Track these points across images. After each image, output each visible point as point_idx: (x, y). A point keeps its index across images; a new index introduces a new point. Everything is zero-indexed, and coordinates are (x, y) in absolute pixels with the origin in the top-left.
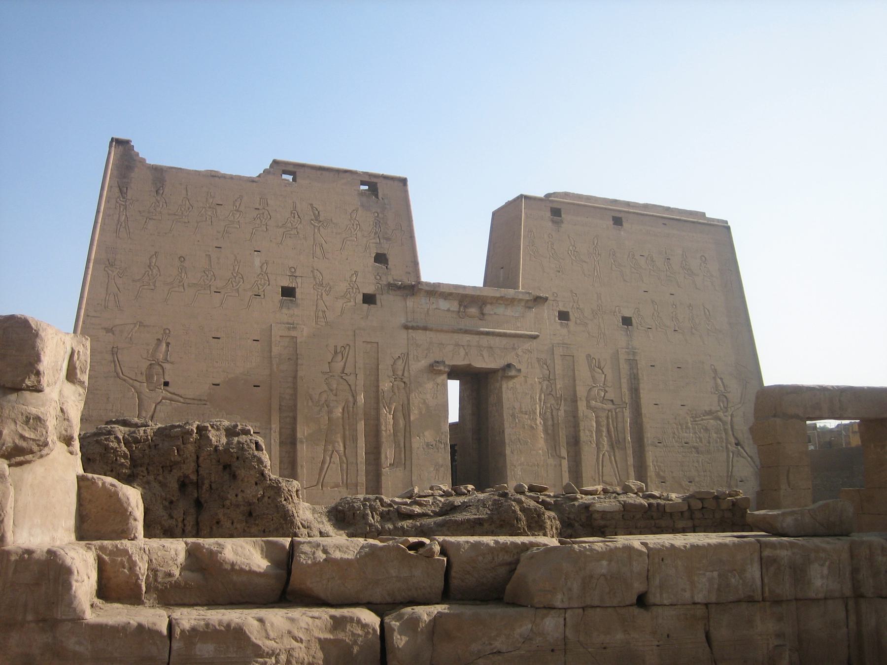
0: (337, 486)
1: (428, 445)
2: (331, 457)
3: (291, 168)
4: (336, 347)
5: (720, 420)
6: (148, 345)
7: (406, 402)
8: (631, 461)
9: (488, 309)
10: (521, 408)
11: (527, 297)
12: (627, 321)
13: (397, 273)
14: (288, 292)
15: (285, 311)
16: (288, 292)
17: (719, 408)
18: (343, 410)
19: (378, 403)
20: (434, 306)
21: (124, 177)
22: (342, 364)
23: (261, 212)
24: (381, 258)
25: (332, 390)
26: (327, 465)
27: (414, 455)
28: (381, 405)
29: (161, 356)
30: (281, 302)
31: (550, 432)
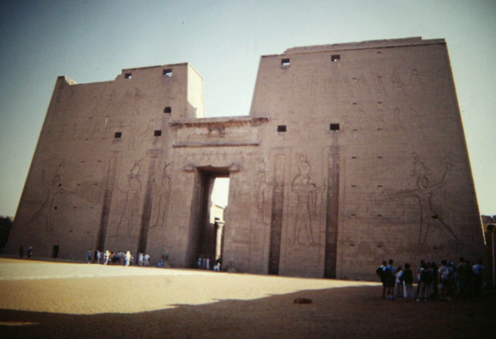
3: (129, 72)
5: (418, 197)
7: (168, 189)
8: (324, 228)
9: (227, 130)
10: (240, 192)
11: (248, 119)
12: (334, 127)
13: (175, 116)
14: (118, 135)
16: (118, 135)
17: (417, 188)
20: (193, 133)
22: (137, 170)
24: (168, 110)
30: (114, 141)
31: (260, 206)
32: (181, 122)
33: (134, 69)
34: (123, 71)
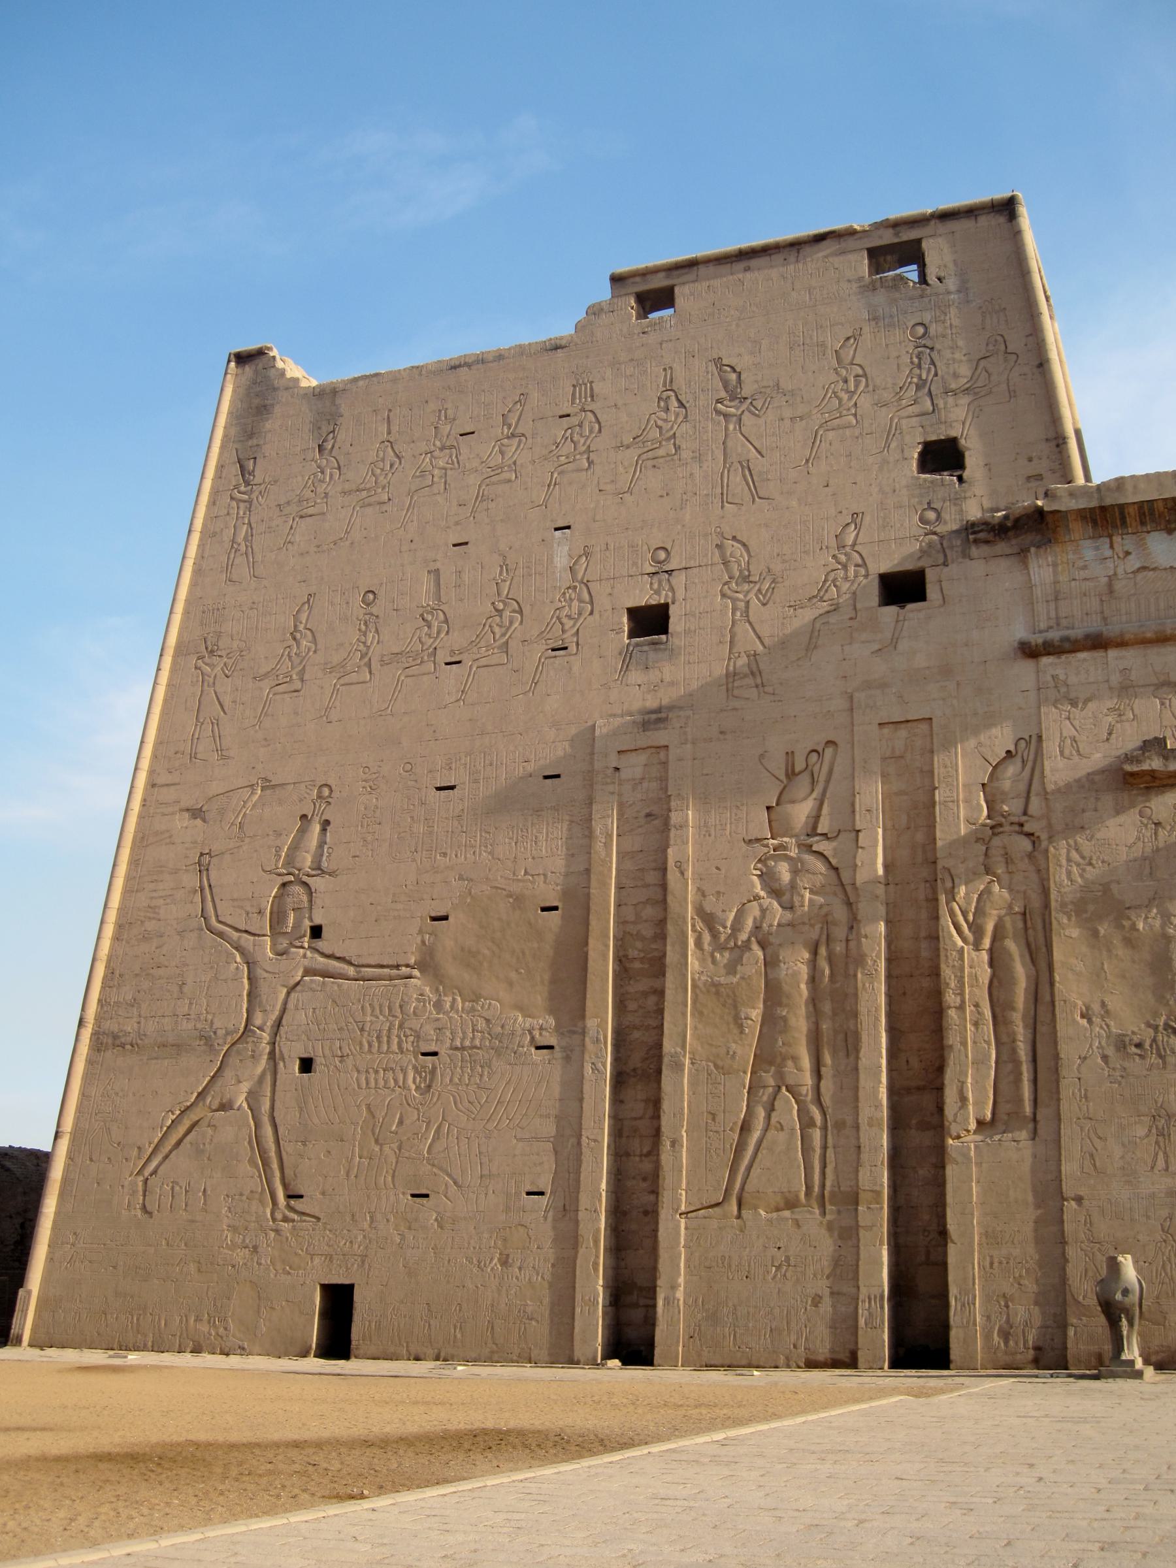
0: (791, 1204)
1: (1121, 1044)
2: (770, 1109)
4: (790, 755)
6: (278, 834)
7: (1036, 904)
14: (650, 622)
15: (635, 676)
16: (650, 622)
18: (815, 953)
19: (936, 918)
20: (1133, 563)
21: (251, 435)
23: (574, 420)
24: (942, 456)
25: (776, 893)
26: (756, 1135)
27: (1068, 1087)
28: (946, 921)
29: (306, 860)
32: (1066, 504)
33: (692, 264)
34: (617, 280)
